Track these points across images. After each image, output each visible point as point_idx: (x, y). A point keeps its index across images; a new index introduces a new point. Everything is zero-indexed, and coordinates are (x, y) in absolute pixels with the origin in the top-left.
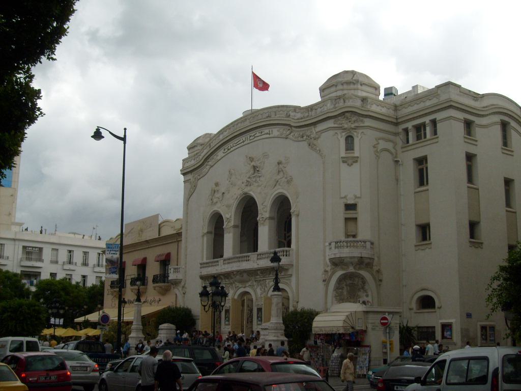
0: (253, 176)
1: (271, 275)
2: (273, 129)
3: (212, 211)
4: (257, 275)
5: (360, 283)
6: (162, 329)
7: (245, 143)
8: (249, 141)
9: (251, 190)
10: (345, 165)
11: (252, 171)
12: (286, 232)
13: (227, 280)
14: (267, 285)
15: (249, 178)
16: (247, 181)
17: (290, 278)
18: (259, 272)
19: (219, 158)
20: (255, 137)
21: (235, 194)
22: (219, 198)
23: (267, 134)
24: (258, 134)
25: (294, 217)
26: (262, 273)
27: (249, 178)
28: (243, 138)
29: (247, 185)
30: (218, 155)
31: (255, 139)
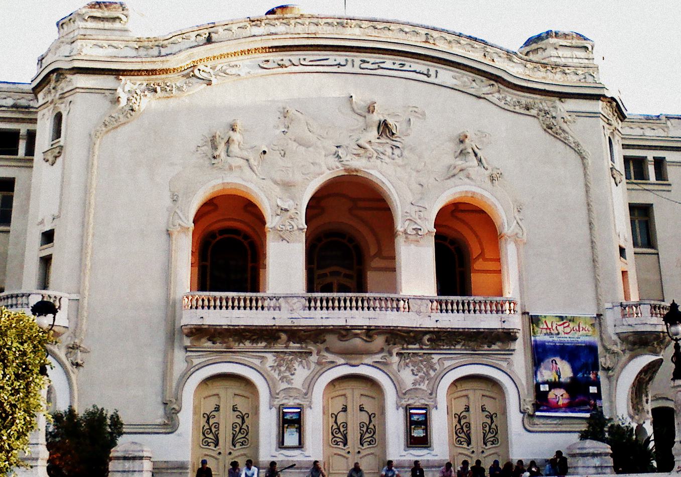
0: (378, 141)
1: (458, 347)
2: (438, 69)
3: (220, 181)
4: (420, 342)
5: (648, 378)
6: (118, 458)
9: (375, 167)
10: (613, 180)
11: (374, 133)
12: (315, 266)
13: (291, 344)
14: (437, 367)
17: (510, 357)
18: (427, 337)
22: (247, 160)
24: (388, 64)
26: (428, 340)
28: (389, 61)
29: (358, 155)
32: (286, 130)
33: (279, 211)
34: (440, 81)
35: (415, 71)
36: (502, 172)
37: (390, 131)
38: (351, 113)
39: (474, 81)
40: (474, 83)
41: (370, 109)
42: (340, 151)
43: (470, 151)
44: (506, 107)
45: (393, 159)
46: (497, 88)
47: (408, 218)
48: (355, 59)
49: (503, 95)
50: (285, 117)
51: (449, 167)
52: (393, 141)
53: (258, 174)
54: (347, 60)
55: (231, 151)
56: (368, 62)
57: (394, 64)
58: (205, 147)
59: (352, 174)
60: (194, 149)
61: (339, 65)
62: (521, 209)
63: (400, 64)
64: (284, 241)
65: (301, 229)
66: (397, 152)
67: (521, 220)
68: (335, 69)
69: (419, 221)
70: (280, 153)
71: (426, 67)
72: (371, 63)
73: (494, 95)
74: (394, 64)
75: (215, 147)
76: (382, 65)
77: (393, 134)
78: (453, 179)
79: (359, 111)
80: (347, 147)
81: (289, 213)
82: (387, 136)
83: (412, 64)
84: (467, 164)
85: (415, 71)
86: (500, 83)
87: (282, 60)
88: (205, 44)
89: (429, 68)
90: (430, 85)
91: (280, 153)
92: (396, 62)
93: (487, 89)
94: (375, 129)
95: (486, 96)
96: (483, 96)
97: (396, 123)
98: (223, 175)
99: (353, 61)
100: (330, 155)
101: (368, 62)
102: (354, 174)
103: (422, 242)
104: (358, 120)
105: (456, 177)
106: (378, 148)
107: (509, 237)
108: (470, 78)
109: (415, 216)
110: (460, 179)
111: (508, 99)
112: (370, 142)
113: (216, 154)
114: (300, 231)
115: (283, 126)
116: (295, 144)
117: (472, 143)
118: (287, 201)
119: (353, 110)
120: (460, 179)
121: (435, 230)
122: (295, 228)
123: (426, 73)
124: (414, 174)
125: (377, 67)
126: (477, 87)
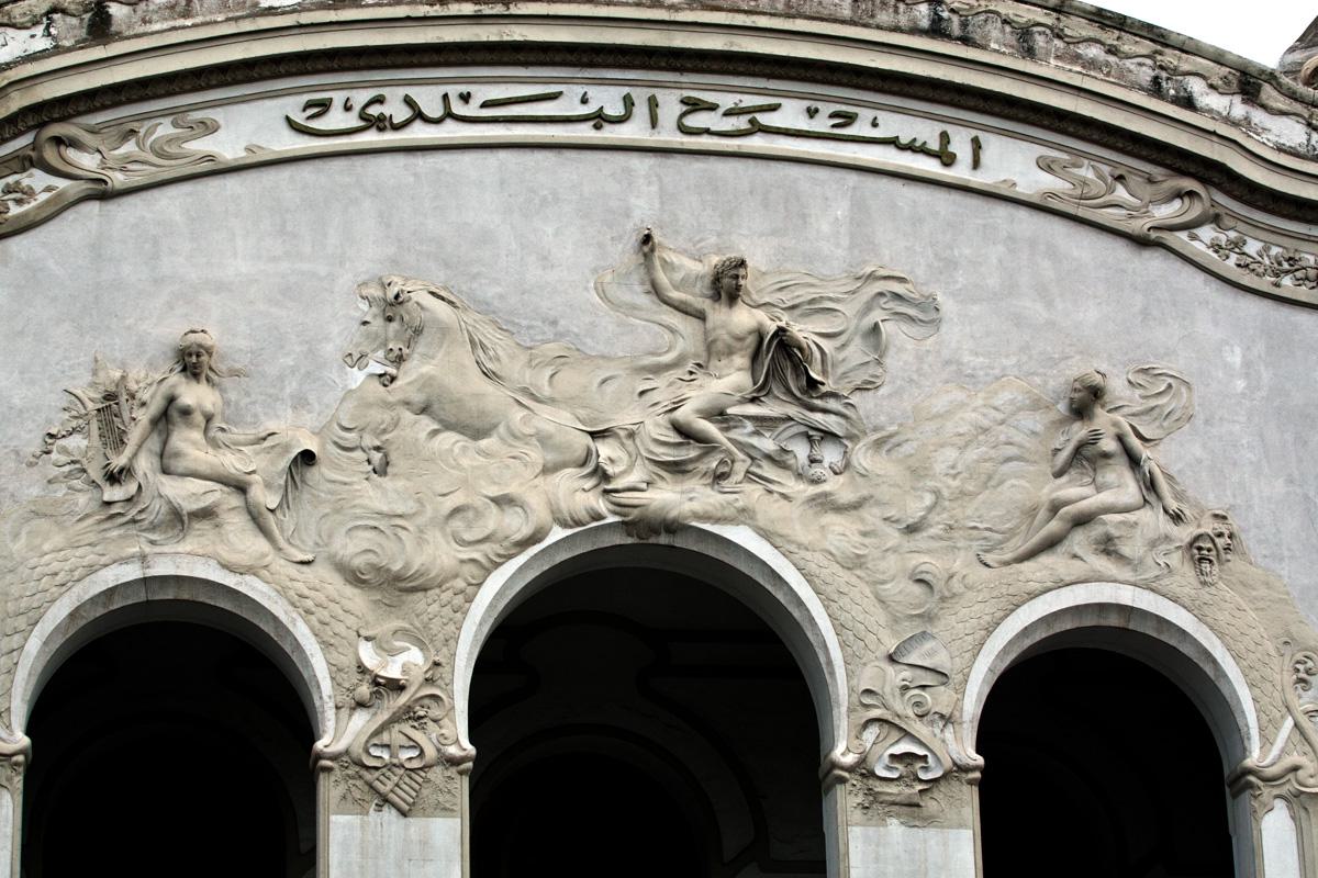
0: (752, 410)
2: (982, 136)
3: (131, 572)
7: (611, 134)
8: (669, 136)
9: (744, 516)
11: (733, 377)
15: (718, 415)
16: (685, 433)
19: (227, 145)
20: (757, 129)
21: (504, 501)
22: (241, 488)
23: (923, 150)
25: (1280, 805)
27: (718, 415)
29: (677, 469)
30: (209, 128)
31: (757, 143)
32: (392, 370)
33: (365, 690)
34: (989, 181)
35: (893, 142)
36: (1235, 529)
37: (800, 368)
38: (645, 301)
39: (1120, 178)
40: (1121, 193)
41: (727, 285)
42: (605, 450)
43: (1108, 444)
44: (1247, 279)
45: (816, 481)
46: (1207, 204)
47: (875, 713)
48: (662, 95)
49: (1232, 235)
50: (390, 319)
51: (1032, 512)
52: (813, 409)
53: (282, 543)
54: (628, 102)
55: (177, 455)
56: (713, 108)
57: (812, 113)
58: (76, 443)
59: (652, 540)
60: (36, 446)
61: (599, 119)
62: (1308, 672)
63: (833, 116)
64: (386, 808)
65: (453, 762)
66: (830, 454)
67: (1310, 714)
68: (584, 133)
69: (920, 729)
70: (369, 462)
71: (939, 127)
72: (721, 111)
73: (1195, 231)
74: (812, 113)
75: (115, 438)
76: (764, 119)
77: (813, 384)
78: (1045, 559)
79: (675, 295)
80: (631, 435)
81: (403, 699)
82: (789, 392)
83: (882, 116)
84: (1106, 498)
85: (893, 142)
86: (1220, 187)
87: (379, 100)
88: (81, 45)
89: (950, 129)
90: (956, 196)
91: (369, 462)
92: (819, 105)
93: (1167, 212)
94: (741, 360)
95: (1169, 238)
96: (1154, 235)
97: (823, 342)
98: (148, 549)
99: (653, 104)
100: (565, 465)
101: (713, 108)
102: (663, 540)
103: (930, 805)
104: (672, 331)
105: (1060, 549)
106: (755, 441)
107: (1266, 780)
108: (1106, 170)
109: (902, 707)
110: (1075, 556)
111: (1253, 247)
112: (722, 413)
113: (119, 461)
114: (453, 772)
115: (380, 354)
116: (427, 424)
117: (1117, 416)
118: (393, 652)
119: (655, 290)
120: (1075, 556)
121: (980, 760)
122: (431, 753)
123: (934, 145)
124: (893, 536)
125: (748, 126)
126: (1132, 199)
